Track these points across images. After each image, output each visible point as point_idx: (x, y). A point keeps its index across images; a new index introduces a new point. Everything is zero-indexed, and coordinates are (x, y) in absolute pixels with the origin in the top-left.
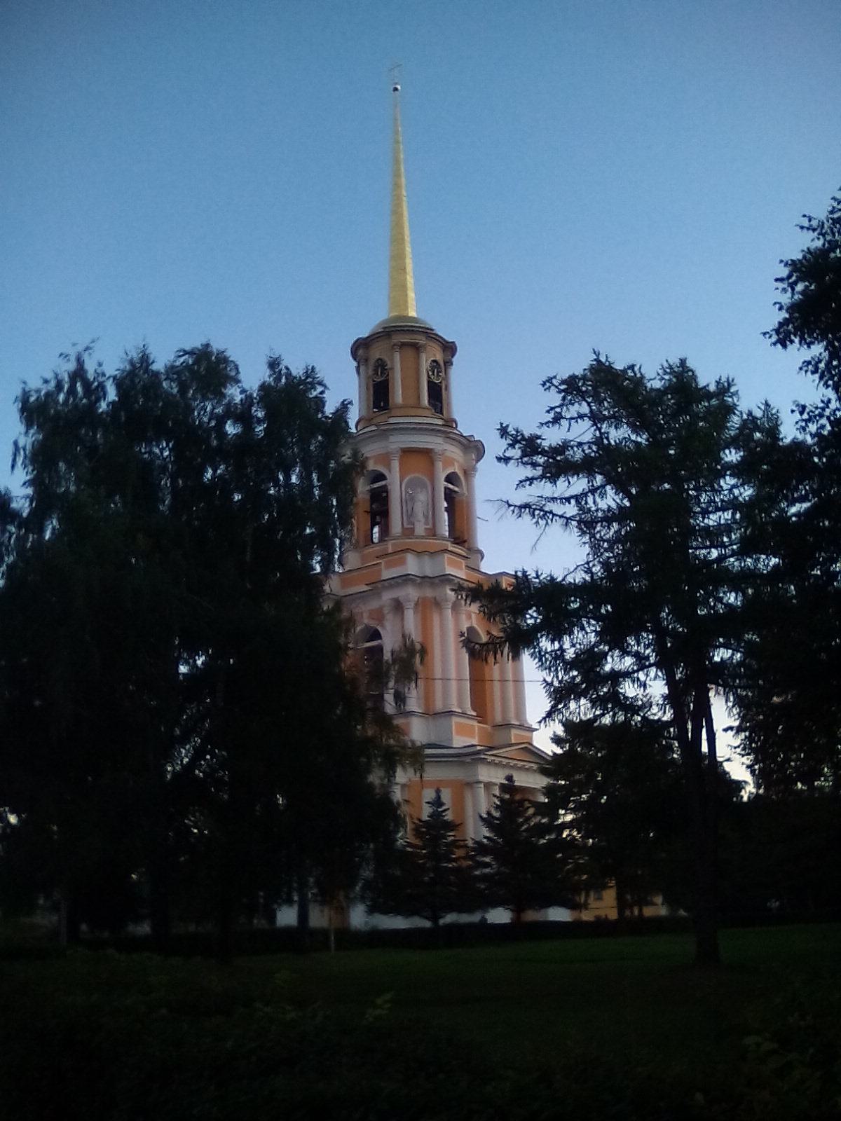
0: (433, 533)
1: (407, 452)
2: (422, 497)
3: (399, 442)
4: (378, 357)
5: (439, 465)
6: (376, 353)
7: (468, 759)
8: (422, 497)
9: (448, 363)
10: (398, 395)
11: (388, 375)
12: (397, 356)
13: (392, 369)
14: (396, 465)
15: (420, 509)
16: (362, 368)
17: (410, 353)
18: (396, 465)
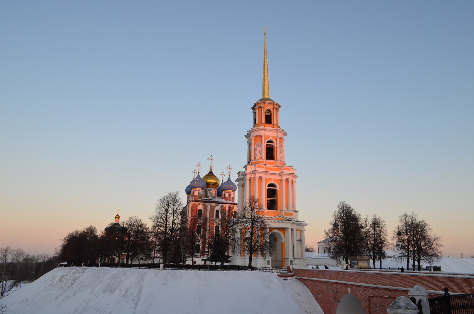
4: (269, 108)
6: (270, 107)
11: (271, 114)
16: (263, 109)
18: (278, 140)
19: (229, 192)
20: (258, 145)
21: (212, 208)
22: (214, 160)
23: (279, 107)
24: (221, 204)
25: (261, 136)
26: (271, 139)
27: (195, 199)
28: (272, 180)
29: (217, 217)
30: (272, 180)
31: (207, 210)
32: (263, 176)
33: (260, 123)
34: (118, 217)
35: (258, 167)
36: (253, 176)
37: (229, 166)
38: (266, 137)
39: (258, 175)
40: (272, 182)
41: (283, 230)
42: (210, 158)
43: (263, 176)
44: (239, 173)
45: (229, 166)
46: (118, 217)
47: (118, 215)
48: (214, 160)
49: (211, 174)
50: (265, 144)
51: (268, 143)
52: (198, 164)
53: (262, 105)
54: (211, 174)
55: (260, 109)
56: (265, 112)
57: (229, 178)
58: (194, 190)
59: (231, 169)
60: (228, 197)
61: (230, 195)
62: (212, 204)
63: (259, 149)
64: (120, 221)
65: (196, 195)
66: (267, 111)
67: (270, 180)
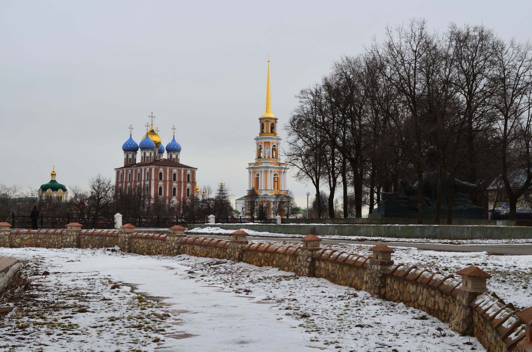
6: (273, 121)
19: (176, 153)
20: (267, 148)
21: (171, 171)
22: (155, 117)
23: (277, 119)
24: (177, 168)
25: (269, 142)
26: (275, 144)
27: (147, 160)
29: (175, 180)
31: (167, 173)
33: (267, 133)
34: (53, 175)
35: (270, 164)
36: (266, 169)
37: (174, 126)
38: (273, 143)
42: (151, 115)
44: (250, 164)
45: (174, 126)
46: (53, 175)
47: (54, 172)
48: (155, 117)
49: (152, 132)
50: (271, 147)
52: (147, 125)
53: (269, 120)
54: (152, 132)
55: (267, 122)
57: (174, 138)
58: (146, 151)
59: (176, 129)
60: (175, 159)
61: (177, 156)
62: (171, 168)
63: (268, 151)
64: (60, 181)
65: (147, 157)
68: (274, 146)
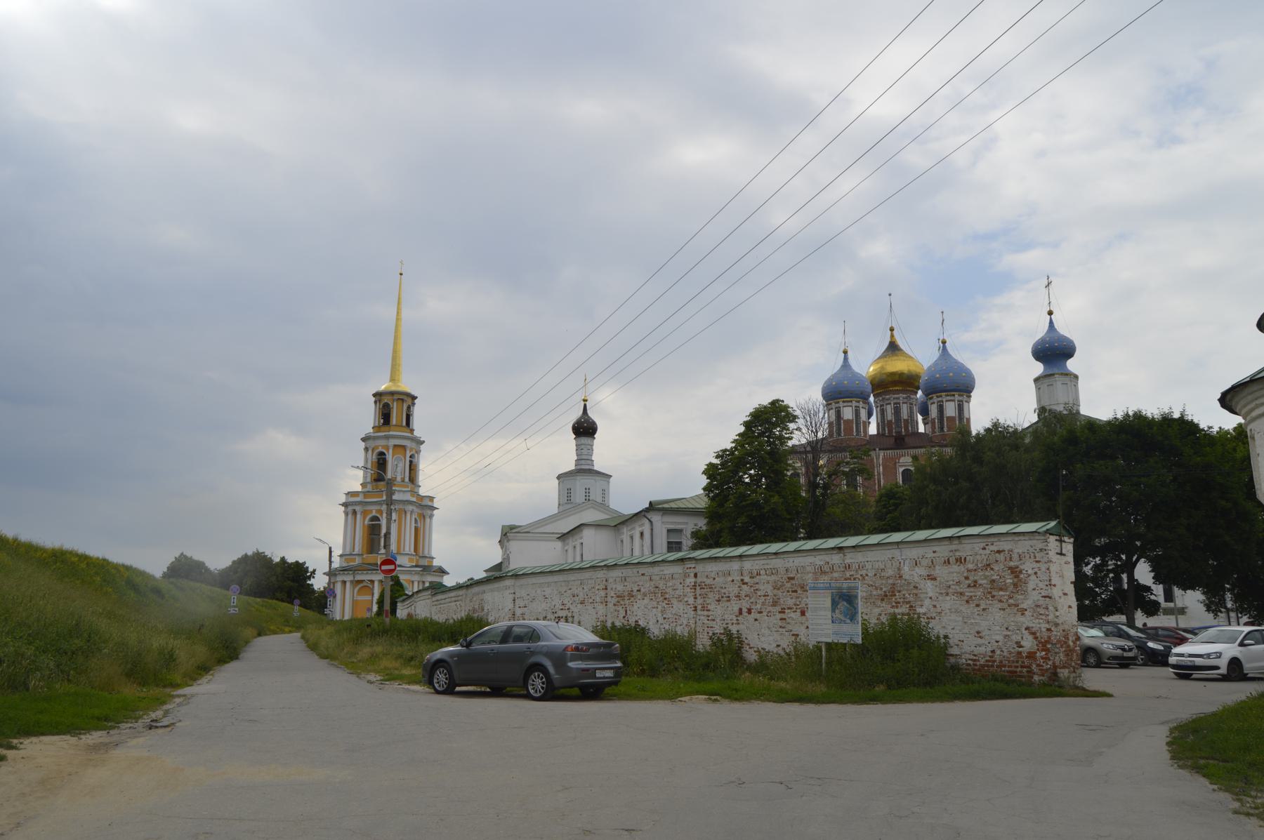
0: (403, 480)
1: (395, 446)
2: (401, 465)
3: (392, 442)
4: (386, 401)
5: (408, 452)
6: (386, 400)
7: (413, 573)
8: (401, 465)
9: (414, 404)
10: (394, 420)
12: (395, 403)
13: (393, 408)
14: (391, 451)
15: (399, 469)
16: (378, 404)
17: (400, 402)
18: (391, 451)
26: (380, 449)
28: (374, 511)
30: (374, 511)
32: (358, 508)
39: (350, 508)
40: (374, 514)
41: (372, 582)
43: (358, 508)
51: (379, 457)
56: (381, 407)
66: (384, 406)
67: (371, 511)
68: (382, 454)
